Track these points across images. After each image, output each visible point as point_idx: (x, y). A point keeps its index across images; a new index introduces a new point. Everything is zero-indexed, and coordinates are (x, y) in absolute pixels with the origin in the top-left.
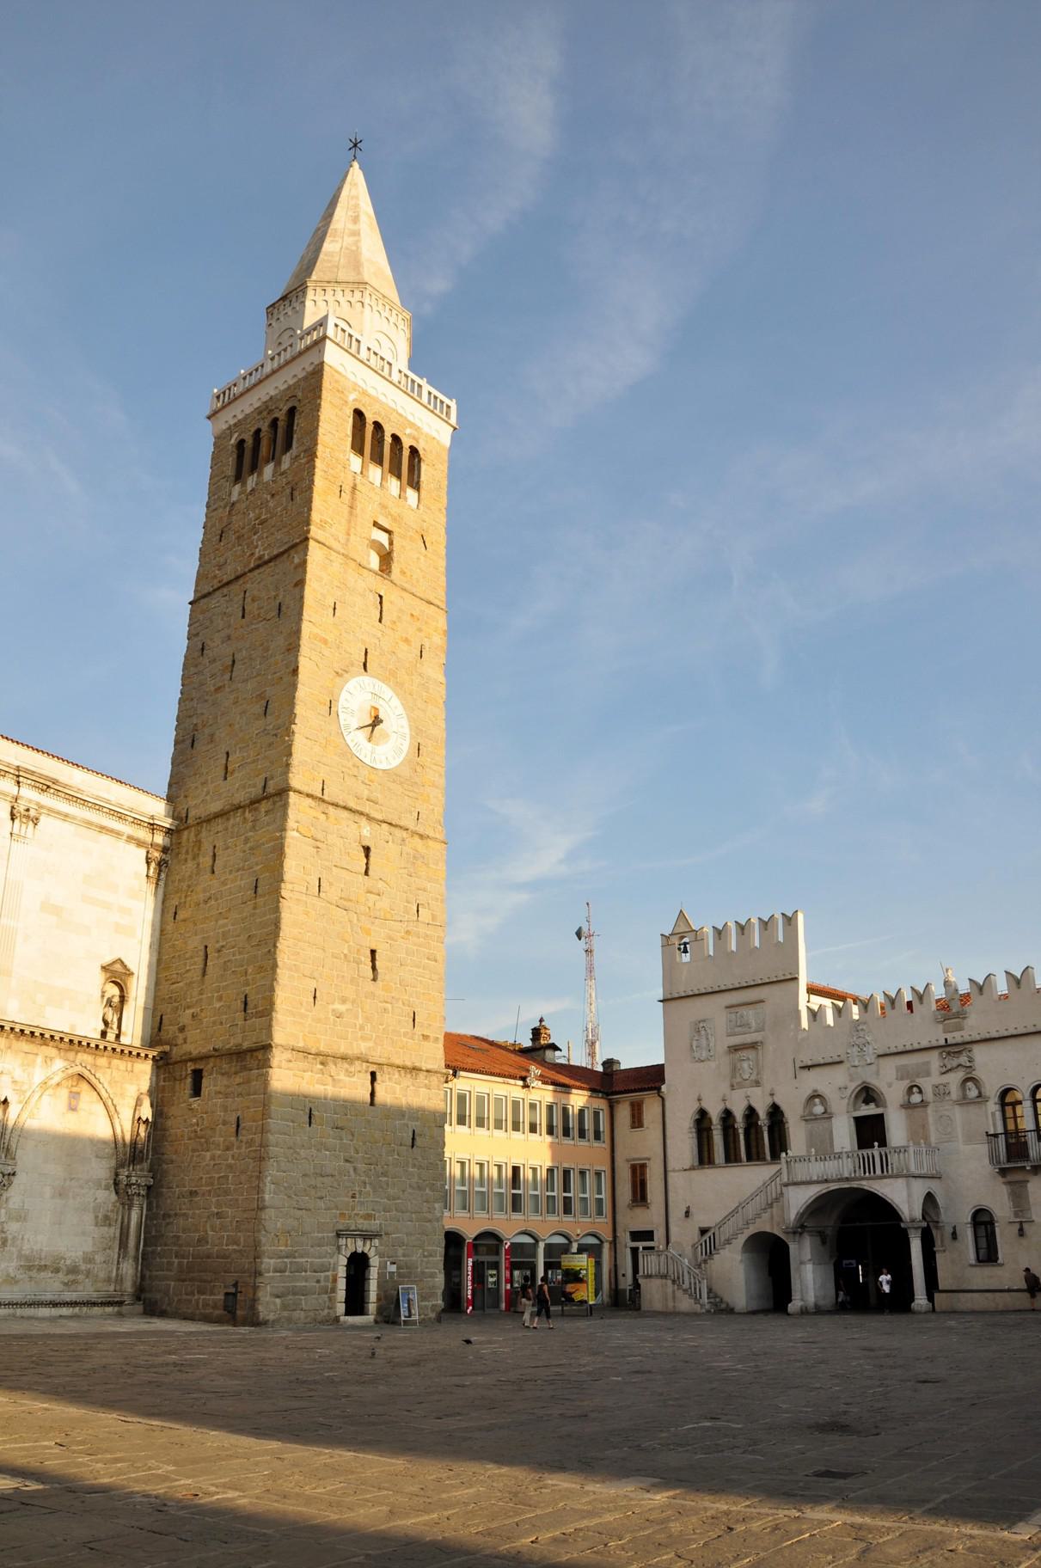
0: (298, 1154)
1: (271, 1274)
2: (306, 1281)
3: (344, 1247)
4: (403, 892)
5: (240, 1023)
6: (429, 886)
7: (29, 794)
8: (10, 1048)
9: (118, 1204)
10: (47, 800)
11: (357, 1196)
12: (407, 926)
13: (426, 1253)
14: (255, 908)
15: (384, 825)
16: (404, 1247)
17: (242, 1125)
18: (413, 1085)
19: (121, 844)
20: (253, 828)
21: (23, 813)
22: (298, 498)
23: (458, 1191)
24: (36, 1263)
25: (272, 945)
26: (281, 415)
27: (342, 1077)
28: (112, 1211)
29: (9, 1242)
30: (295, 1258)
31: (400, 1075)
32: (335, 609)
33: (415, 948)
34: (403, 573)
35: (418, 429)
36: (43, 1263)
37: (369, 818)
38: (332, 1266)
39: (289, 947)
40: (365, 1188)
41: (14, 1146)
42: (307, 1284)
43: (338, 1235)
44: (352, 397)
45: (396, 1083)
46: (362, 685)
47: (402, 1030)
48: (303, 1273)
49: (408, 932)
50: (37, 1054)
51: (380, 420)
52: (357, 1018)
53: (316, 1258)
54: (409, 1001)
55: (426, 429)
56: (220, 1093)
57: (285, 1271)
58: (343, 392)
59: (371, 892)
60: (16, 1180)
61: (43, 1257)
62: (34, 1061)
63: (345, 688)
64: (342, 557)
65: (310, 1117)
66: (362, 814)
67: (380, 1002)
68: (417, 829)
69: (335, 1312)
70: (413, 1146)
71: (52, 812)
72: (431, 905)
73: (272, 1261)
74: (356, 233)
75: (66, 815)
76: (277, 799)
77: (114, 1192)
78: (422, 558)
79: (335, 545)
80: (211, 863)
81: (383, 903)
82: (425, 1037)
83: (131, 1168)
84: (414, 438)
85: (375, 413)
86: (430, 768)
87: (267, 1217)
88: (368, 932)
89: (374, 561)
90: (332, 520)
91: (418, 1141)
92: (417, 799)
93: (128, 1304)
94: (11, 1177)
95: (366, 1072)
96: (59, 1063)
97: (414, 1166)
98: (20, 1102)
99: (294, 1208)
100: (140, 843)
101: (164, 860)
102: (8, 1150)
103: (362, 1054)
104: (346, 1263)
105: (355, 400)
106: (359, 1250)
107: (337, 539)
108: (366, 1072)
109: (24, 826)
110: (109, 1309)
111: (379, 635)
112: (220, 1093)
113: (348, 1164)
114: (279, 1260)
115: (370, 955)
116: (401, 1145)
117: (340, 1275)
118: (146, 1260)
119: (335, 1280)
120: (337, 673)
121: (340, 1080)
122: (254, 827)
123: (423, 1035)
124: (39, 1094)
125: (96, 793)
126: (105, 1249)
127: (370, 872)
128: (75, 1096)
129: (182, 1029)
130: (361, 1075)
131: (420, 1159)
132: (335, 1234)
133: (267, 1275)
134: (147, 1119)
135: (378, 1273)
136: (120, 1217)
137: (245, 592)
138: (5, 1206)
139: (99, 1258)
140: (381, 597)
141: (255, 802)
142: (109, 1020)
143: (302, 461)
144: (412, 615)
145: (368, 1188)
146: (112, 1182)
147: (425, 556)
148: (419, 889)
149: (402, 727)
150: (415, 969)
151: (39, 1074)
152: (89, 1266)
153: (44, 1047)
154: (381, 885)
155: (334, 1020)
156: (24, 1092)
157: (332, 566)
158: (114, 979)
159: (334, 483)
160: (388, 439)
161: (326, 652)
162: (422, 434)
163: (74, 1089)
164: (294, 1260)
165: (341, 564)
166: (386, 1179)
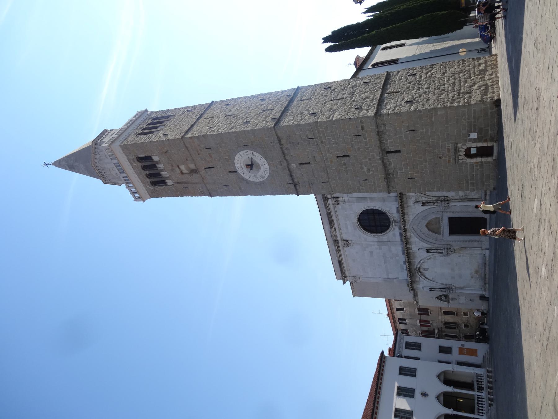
1: (475, 188)
2: (478, 175)
3: (463, 161)
11: (440, 156)
18: (386, 132)
27: (392, 166)
30: (468, 179)
31: (383, 140)
40: (436, 152)
42: (479, 174)
44: (152, 188)
48: (475, 175)
50: (406, 195)
53: (468, 172)
59: (315, 160)
63: (249, 179)
73: (470, 188)
82: (363, 128)
84: (134, 161)
88: (331, 162)
91: (411, 129)
95: (387, 156)
103: (380, 158)
104: (470, 159)
105: (150, 186)
108: (387, 156)
109: (340, 201)
114: (470, 185)
117: (475, 161)
123: (362, 130)
135: (474, 142)
144: (199, 154)
156: (418, 197)
160: (147, 172)
164: (469, 180)
166: (431, 143)
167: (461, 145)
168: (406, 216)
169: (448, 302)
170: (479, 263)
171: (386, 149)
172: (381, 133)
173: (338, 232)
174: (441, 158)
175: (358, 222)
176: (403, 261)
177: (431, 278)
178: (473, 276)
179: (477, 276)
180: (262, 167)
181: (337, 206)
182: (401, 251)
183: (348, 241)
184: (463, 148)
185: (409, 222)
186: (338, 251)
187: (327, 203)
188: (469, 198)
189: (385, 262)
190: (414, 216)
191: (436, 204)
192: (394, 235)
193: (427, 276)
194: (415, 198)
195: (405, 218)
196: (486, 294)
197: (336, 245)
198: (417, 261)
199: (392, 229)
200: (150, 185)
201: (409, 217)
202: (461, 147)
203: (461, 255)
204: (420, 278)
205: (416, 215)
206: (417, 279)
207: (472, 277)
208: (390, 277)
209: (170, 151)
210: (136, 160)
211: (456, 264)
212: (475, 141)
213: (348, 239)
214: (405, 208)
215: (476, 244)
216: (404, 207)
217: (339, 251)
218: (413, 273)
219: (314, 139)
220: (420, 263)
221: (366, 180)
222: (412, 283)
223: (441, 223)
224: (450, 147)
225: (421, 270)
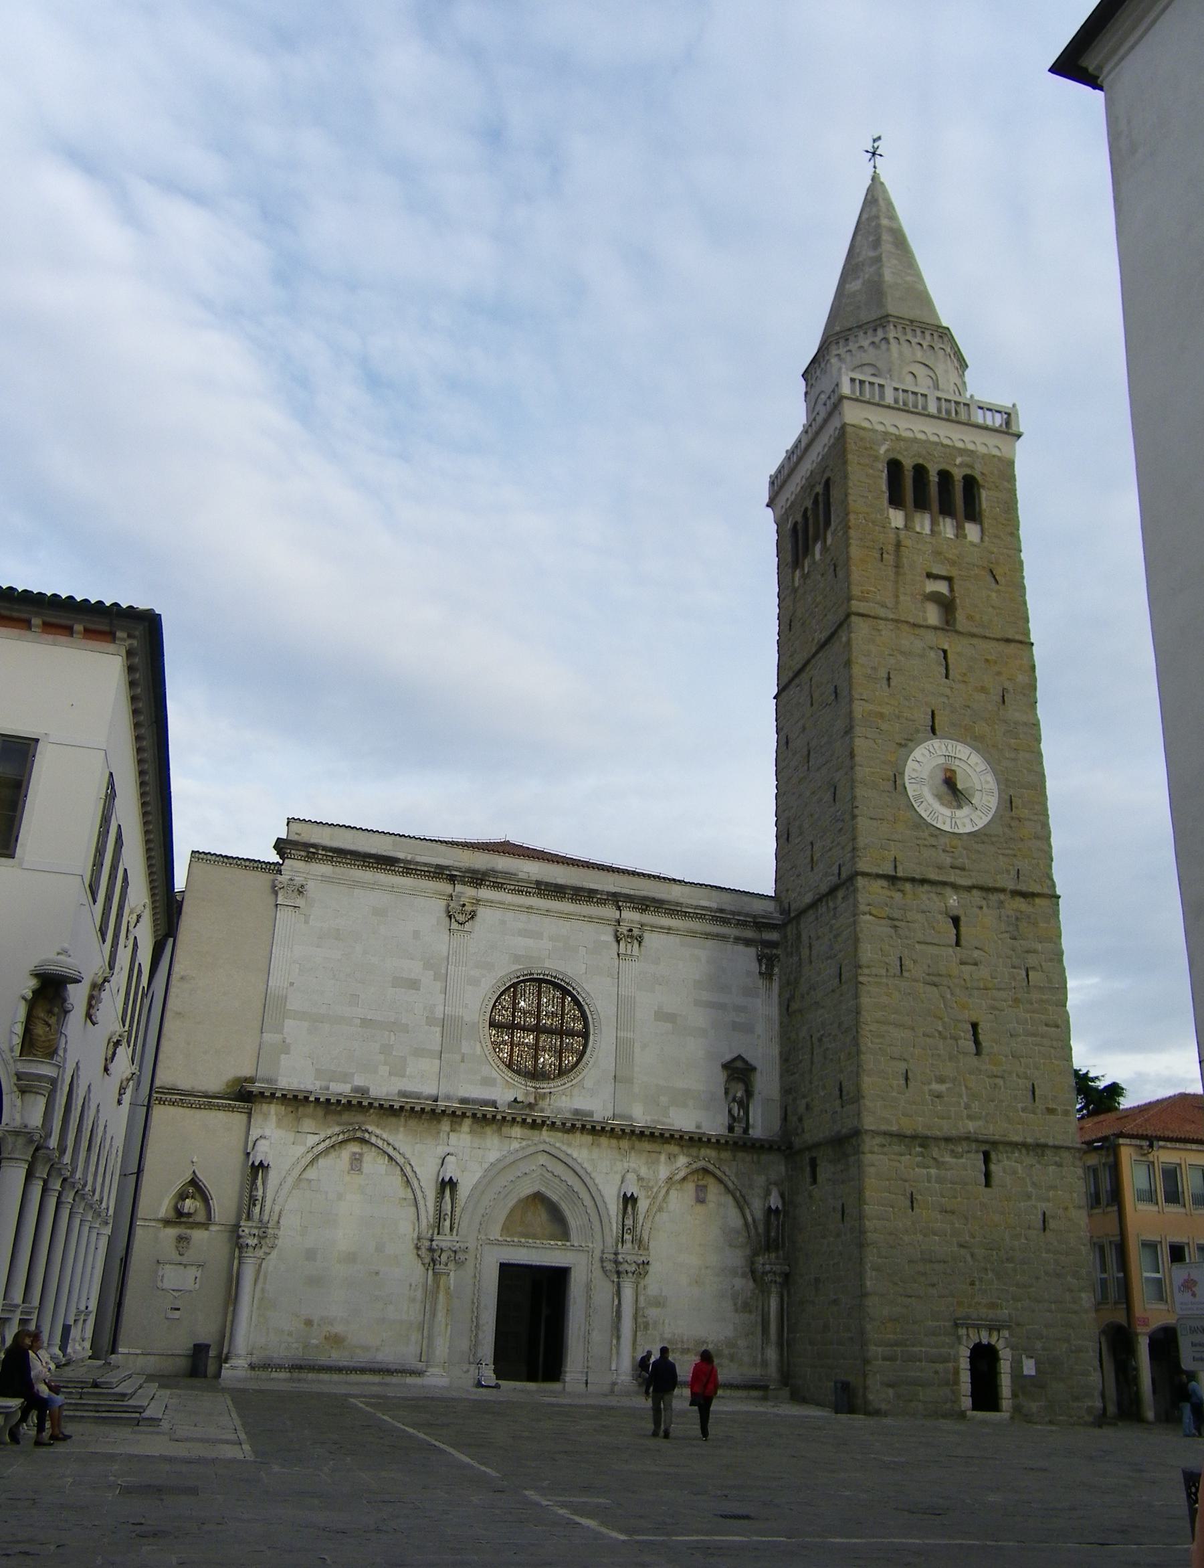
0: (901, 1238)
3: (965, 1337)
4: (1008, 957)
5: (839, 1109)
6: (1039, 947)
7: (631, 916)
8: (633, 1148)
9: (757, 1291)
10: (648, 918)
11: (977, 1283)
12: (1015, 993)
13: (1073, 1348)
14: (841, 995)
15: (975, 892)
16: (1044, 1340)
17: (846, 1212)
18: (1039, 1162)
19: (729, 946)
20: (835, 917)
21: (625, 932)
22: (841, 574)
23: (1147, 1279)
24: (679, 1346)
25: (855, 1030)
26: (819, 489)
27: (948, 1159)
28: (751, 1298)
29: (651, 1326)
30: (906, 1346)
31: (1020, 1151)
32: (889, 679)
33: (1028, 1016)
34: (970, 618)
35: (971, 453)
36: (685, 1346)
37: (955, 887)
38: (952, 1357)
39: (871, 1031)
40: (987, 1275)
41: (646, 1237)
43: (956, 1325)
44: (882, 451)
45: (1016, 1162)
46: (932, 750)
47: (1020, 1105)
48: (918, 1363)
49: (1016, 1000)
51: (921, 461)
52: (960, 1096)
54: (1025, 1073)
55: (982, 450)
56: (830, 1180)
57: (896, 1360)
58: (871, 448)
60: (652, 1269)
61: (685, 1339)
62: (658, 1161)
63: (911, 758)
64: (891, 623)
65: (912, 1202)
66: (944, 884)
67: (988, 1077)
68: (1018, 888)
69: (960, 1408)
70: (1044, 1229)
71: (654, 928)
72: (1044, 967)
73: (880, 1349)
74: (878, 260)
75: (669, 929)
76: (848, 884)
77: (751, 1281)
78: (994, 595)
79: (882, 612)
80: (808, 954)
81: (984, 972)
82: (1051, 1111)
83: (766, 1257)
85: (914, 456)
86: (1030, 820)
87: (871, 1304)
89: (933, 615)
90: (876, 588)
92: (1015, 856)
93: (774, 1389)
94: (647, 1267)
95: (977, 1152)
96: (682, 1160)
97: (1048, 1251)
98: (648, 1197)
99: (901, 1295)
100: (748, 942)
101: (775, 954)
102: (640, 1241)
104: (968, 1354)
105: (887, 451)
106: (985, 1341)
107: (884, 606)
110: (754, 1393)
111: (948, 691)
112: (830, 1180)
113: (963, 1251)
115: (970, 1028)
116: (1029, 1228)
117: (962, 1366)
118: (785, 1345)
119: (957, 1372)
120: (900, 745)
121: (943, 1163)
122: (835, 914)
124: (665, 1189)
125: (695, 903)
126: (747, 1335)
127: (963, 942)
128: (701, 1190)
129: (800, 1120)
130: (972, 1155)
131: (1056, 1244)
132: (951, 1323)
133: (874, 1362)
134: (777, 1208)
136: (760, 1304)
137: (811, 680)
138: (643, 1292)
139: (741, 1343)
140: (945, 652)
141: (833, 891)
142: (736, 1115)
143: (840, 534)
144: (987, 661)
145: (990, 1275)
146: (748, 1270)
147: (998, 591)
148: (1027, 952)
149: (987, 782)
150: (1030, 1039)
151: (663, 1171)
152: (732, 1351)
153: (666, 1146)
154: (976, 954)
155: (932, 1100)
156: (652, 1187)
157: (881, 635)
158: (736, 1075)
159: (874, 548)
160: (934, 478)
161: (884, 726)
162: (978, 457)
163: (701, 1183)
165: (892, 630)
167: (1007, 1336)
168: (589, 1138)
169: (167, 1222)
170: (377, 1349)
171: (997, 1155)
172: (1040, 1152)
173: (509, 898)
174: (972, 1284)
175: (541, 977)
176: (368, 1089)
177: (311, 1174)
178: (315, 1326)
179: (314, 1341)
180: (947, 812)
181: (610, 930)
182: (416, 1090)
183: (473, 916)
184: (998, 1340)
185: (563, 1142)
186: (439, 873)
187: (628, 905)
188: (638, 1333)
189: (366, 1022)
190: (585, 1165)
191: (627, 1237)
192: (487, 1082)
193: (322, 1161)
194: (649, 1180)
195: (582, 1133)
196: (233, 1368)
197: (467, 875)
198: (400, 1138)
199: (509, 1080)
200: (892, 456)
201: (581, 1146)
202: (1001, 1335)
203: (419, 1294)
204: (316, 1138)
205: (589, 1169)
206: (308, 1125)
207: (309, 1323)
208: (289, 1023)
209: (993, 585)
210: (969, 472)
211: (377, 1273)
212: (1017, 1365)
213: (478, 918)
214: (614, 1142)
215: (464, 1345)
216: (619, 1138)
217: (432, 874)
218: (340, 1113)
219: (1025, 984)
220: (390, 1150)
221: (907, 1079)
222: (296, 1101)
223: (552, 1242)
224: (1002, 1309)
225: (355, 1148)
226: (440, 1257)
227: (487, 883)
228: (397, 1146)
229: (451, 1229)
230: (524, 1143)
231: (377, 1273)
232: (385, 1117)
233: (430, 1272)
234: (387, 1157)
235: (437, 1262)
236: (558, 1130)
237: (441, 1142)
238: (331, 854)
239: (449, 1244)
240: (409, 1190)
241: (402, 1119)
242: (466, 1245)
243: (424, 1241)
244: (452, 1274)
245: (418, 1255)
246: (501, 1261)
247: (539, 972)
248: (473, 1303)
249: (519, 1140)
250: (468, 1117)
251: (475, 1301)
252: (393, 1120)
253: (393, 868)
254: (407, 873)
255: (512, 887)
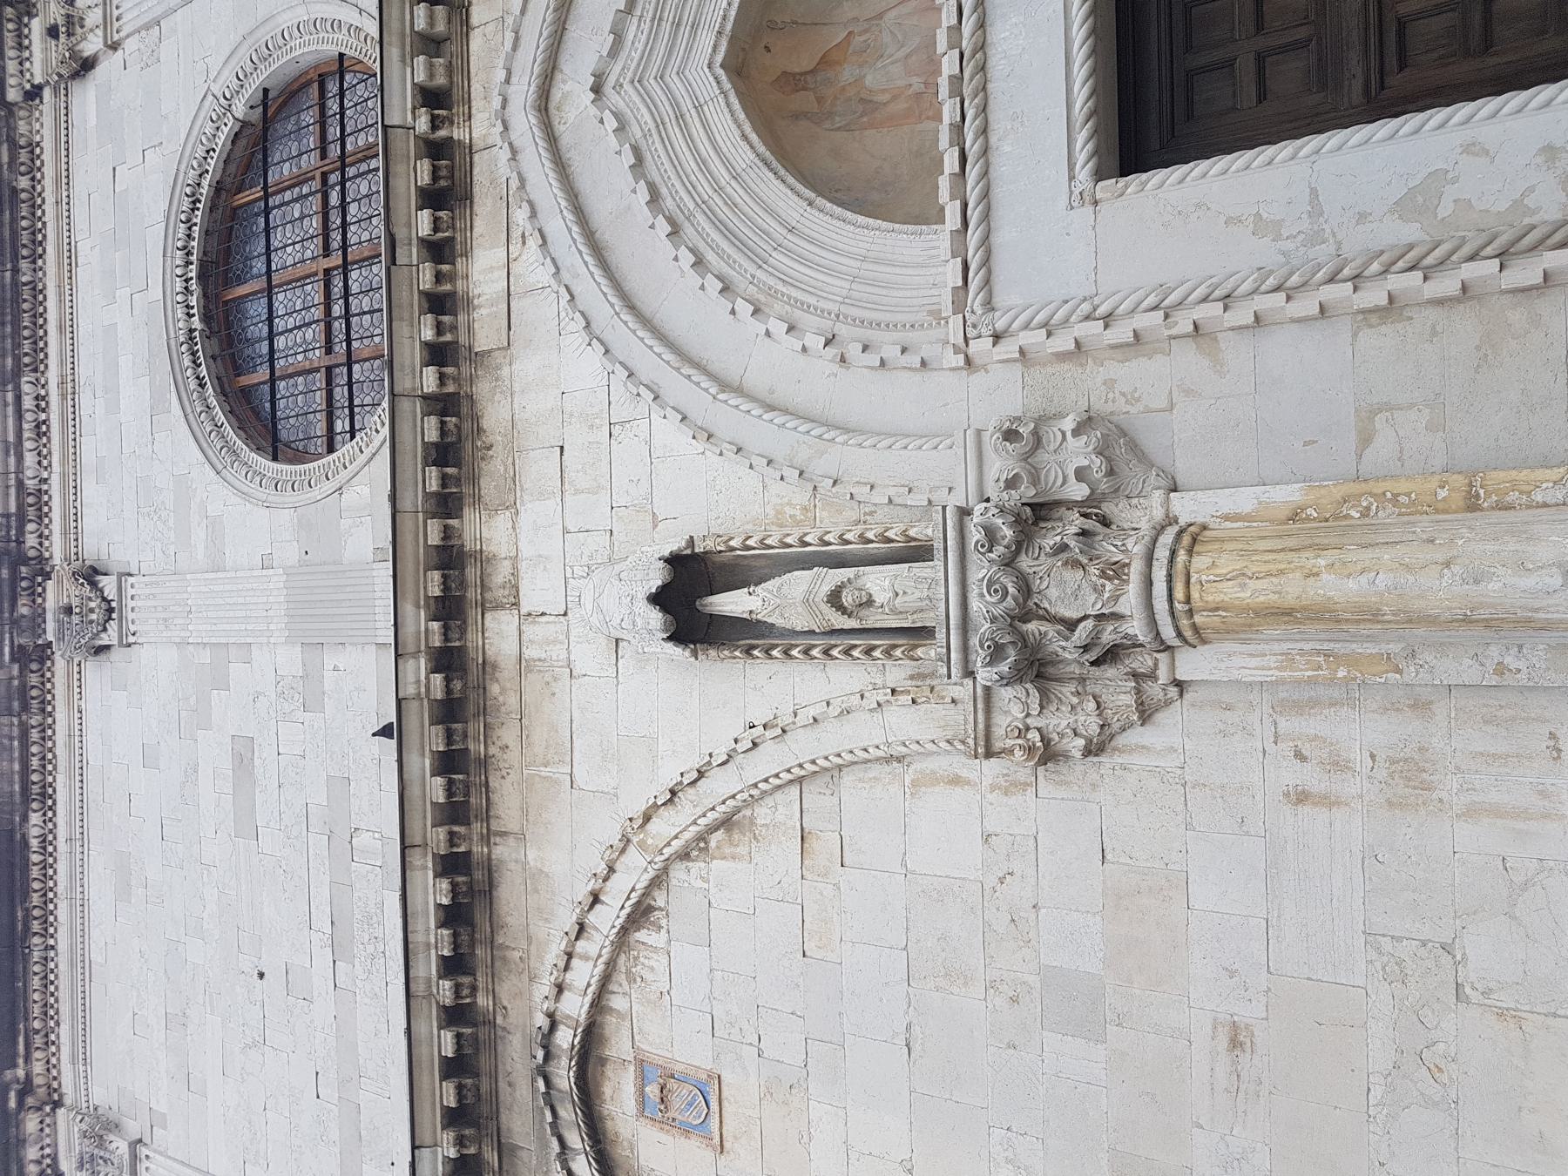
187: (12, 67)
220: (607, 919)
226: (1071, 625)
227: (31, 540)
228: (582, 892)
229: (917, 553)
230: (521, 215)
231: (1235, 1043)
232: (500, 940)
233: (1191, 664)
234: (641, 935)
235: (1108, 636)
236: (460, 68)
237: (558, 653)
238: (21, 1040)
239: (980, 570)
240: (762, 813)
241: (501, 851)
242: (991, 440)
243: (1001, 723)
244: (1186, 508)
245: (1094, 749)
246: (1084, 174)
247: (180, 313)
248: (1393, 307)
249: (515, 249)
250: (447, 533)
251: (1374, 296)
252: (509, 894)
253: (34, 843)
254: (43, 795)
255: (30, 459)
